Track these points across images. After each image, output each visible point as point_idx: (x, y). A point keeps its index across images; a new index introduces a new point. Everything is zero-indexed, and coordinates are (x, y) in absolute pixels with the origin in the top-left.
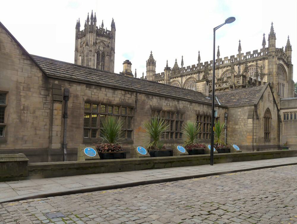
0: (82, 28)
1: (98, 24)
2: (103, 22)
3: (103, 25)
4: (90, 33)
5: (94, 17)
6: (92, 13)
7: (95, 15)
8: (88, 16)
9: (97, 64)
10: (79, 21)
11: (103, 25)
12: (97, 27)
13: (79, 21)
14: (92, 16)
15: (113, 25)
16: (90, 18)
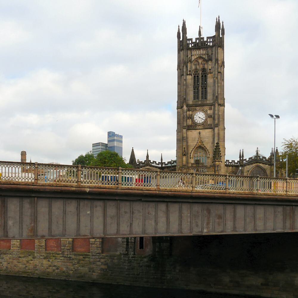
7: (223, 25)
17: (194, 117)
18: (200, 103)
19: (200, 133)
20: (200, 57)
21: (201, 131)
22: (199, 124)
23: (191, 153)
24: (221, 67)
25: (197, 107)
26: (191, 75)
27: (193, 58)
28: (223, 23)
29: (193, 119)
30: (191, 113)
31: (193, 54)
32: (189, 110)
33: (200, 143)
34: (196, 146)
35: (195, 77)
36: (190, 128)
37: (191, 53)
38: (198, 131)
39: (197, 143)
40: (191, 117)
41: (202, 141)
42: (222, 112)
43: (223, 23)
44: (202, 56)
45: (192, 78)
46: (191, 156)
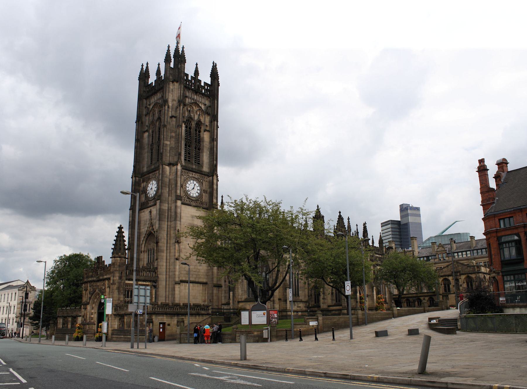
0: (152, 79)
1: (189, 70)
2: (197, 68)
3: (197, 72)
4: (173, 82)
5: (180, 52)
6: (177, 46)
7: (183, 51)
8: (169, 50)
9: (186, 145)
10: (147, 67)
11: (197, 72)
12: (187, 75)
13: (147, 67)
14: (177, 50)
15: (214, 75)
16: (172, 56)
17: (147, 189)
18: (153, 167)
19: (150, 212)
20: (156, 104)
21: (151, 208)
22: (151, 199)
23: (142, 244)
24: (177, 108)
25: (150, 175)
26: (147, 131)
27: (151, 107)
28: (183, 48)
29: (147, 192)
30: (145, 183)
31: (152, 102)
32: (143, 182)
33: (151, 228)
34: (147, 233)
35: (153, 132)
36: (144, 206)
37: (150, 102)
38: (149, 209)
39: (148, 228)
40: (145, 191)
41: (153, 223)
42: (175, 173)
43: (183, 48)
44: (158, 102)
45: (149, 136)
46: (143, 249)
